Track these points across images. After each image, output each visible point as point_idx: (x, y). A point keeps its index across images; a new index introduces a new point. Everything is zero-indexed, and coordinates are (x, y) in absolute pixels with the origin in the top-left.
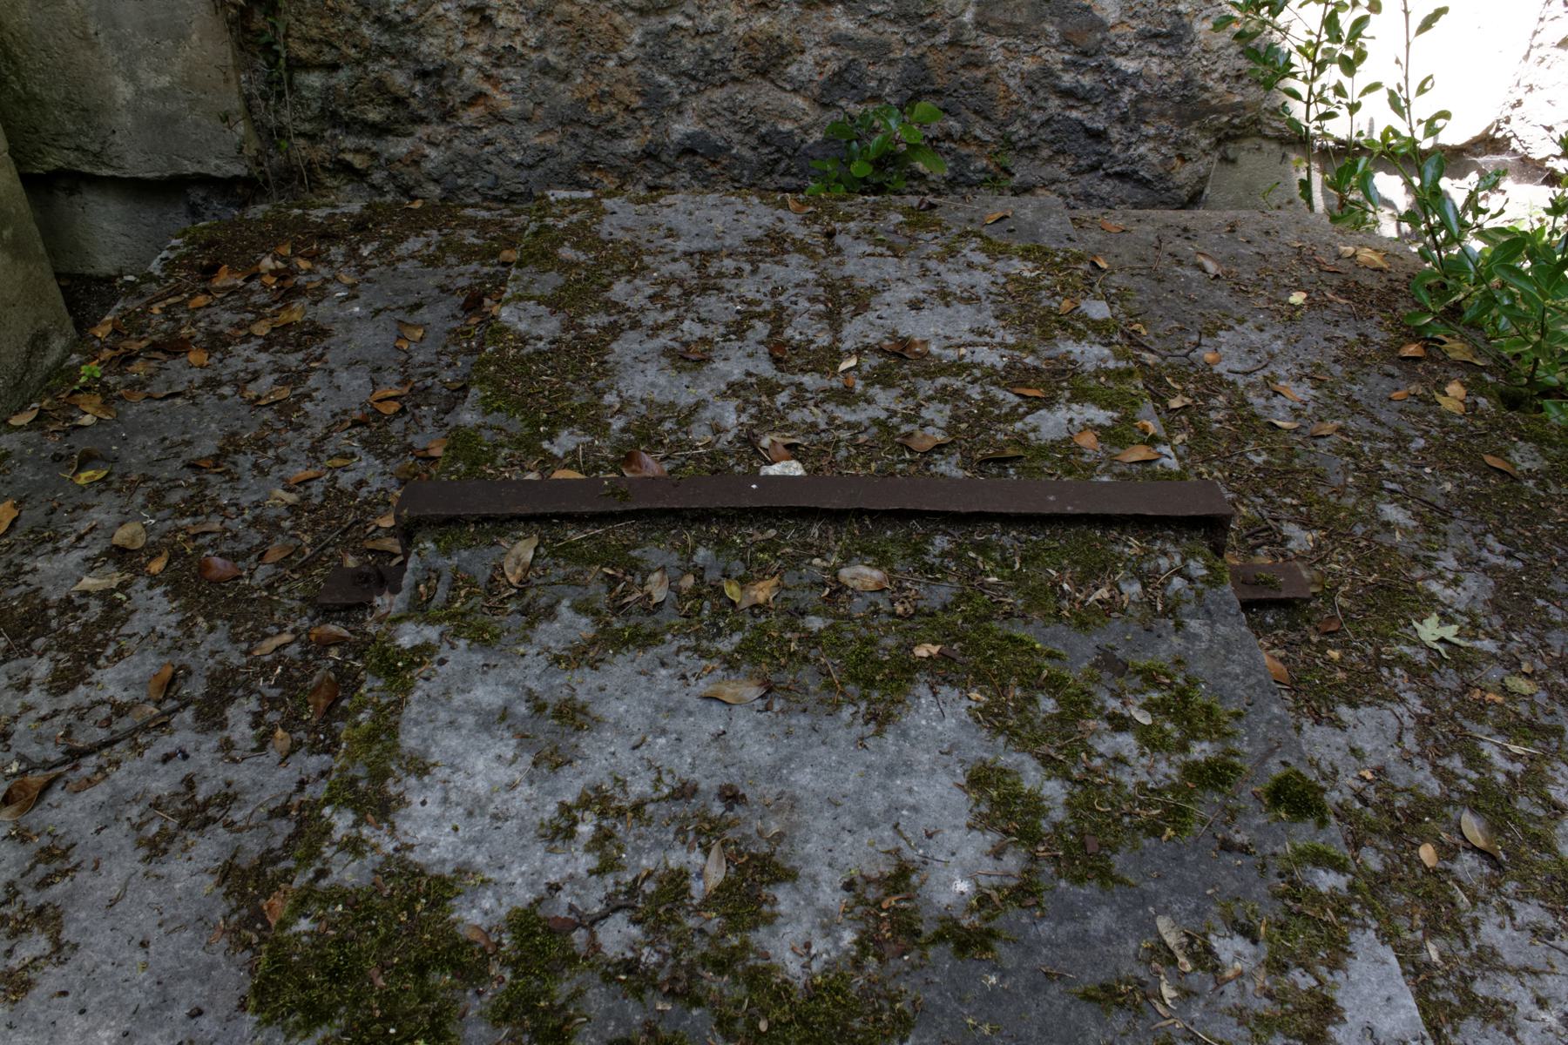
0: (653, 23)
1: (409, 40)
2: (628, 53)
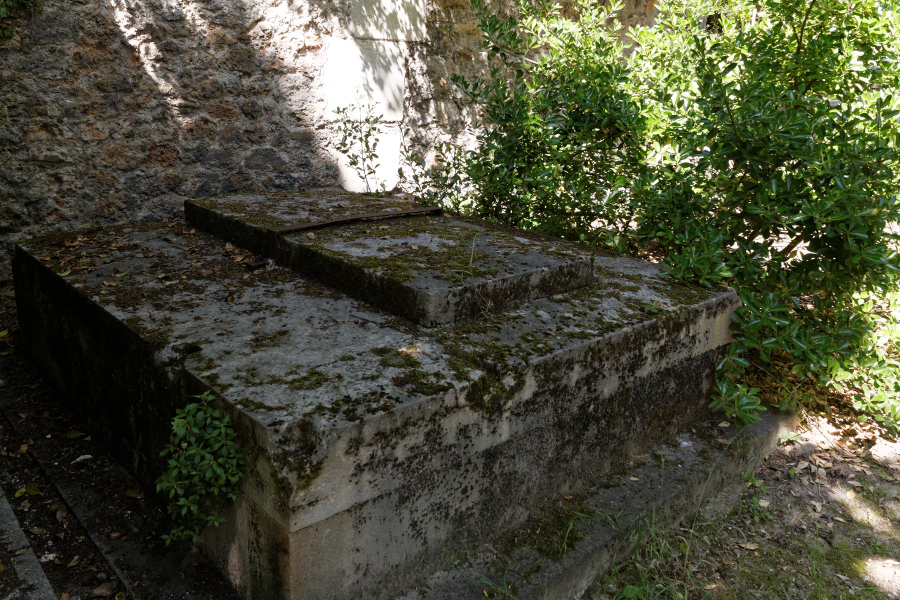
0: (129, 175)
1: (23, 190)
2: (120, 187)
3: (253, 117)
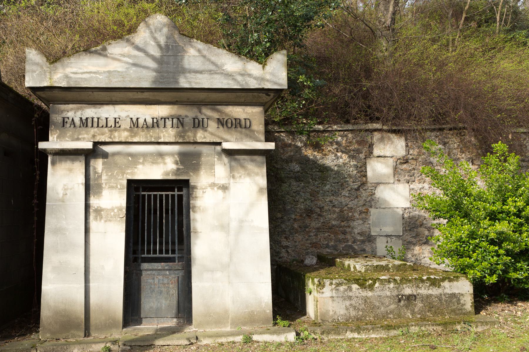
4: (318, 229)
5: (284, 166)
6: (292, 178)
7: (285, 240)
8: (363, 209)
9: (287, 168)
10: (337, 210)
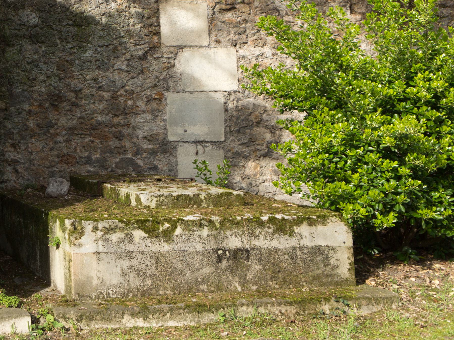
3: (120, 140)
4: (72, 130)
5: (10, 16)
6: (24, 36)
7: (12, 149)
8: (154, 93)
9: (16, 19)
10: (106, 95)
